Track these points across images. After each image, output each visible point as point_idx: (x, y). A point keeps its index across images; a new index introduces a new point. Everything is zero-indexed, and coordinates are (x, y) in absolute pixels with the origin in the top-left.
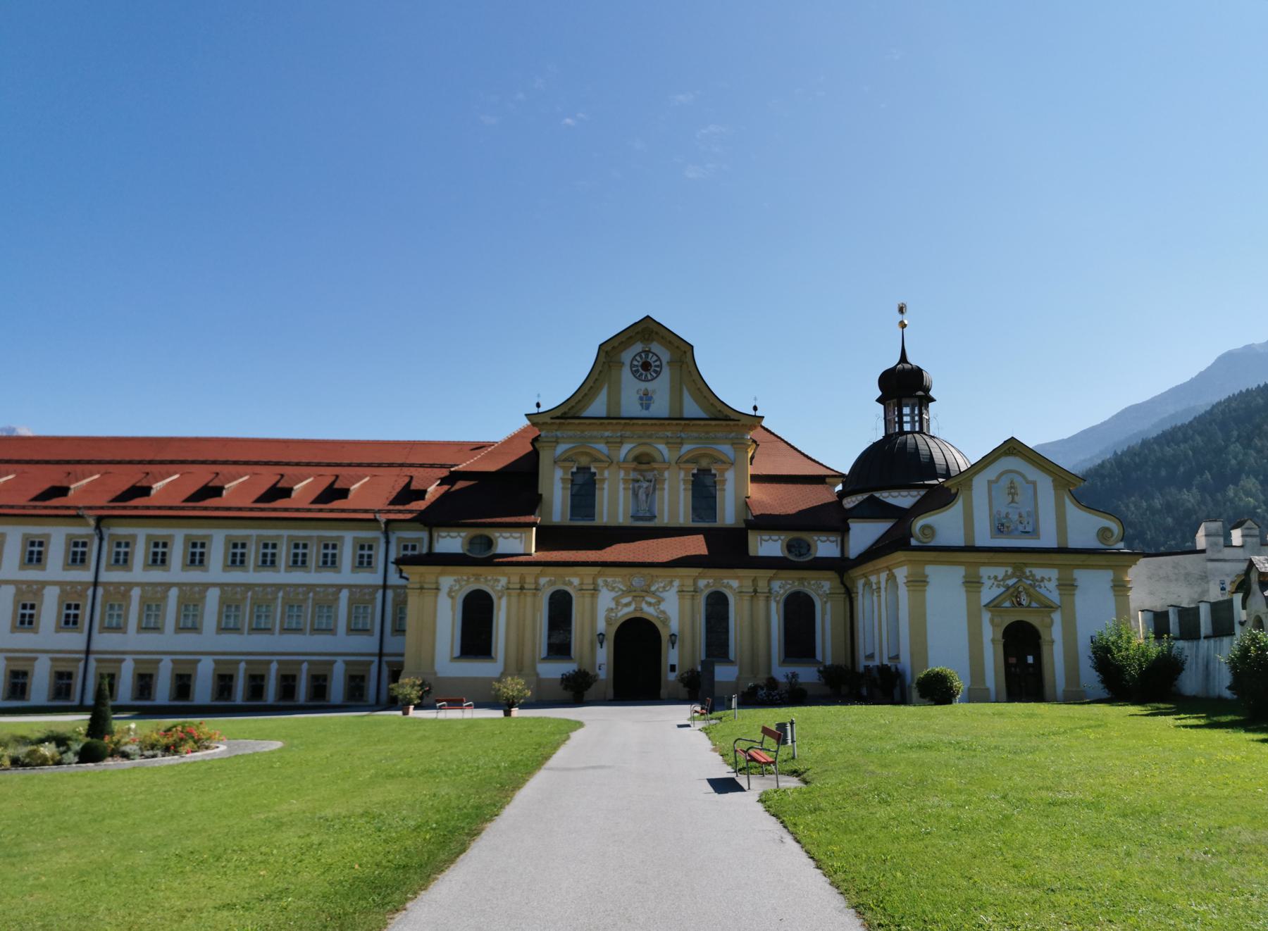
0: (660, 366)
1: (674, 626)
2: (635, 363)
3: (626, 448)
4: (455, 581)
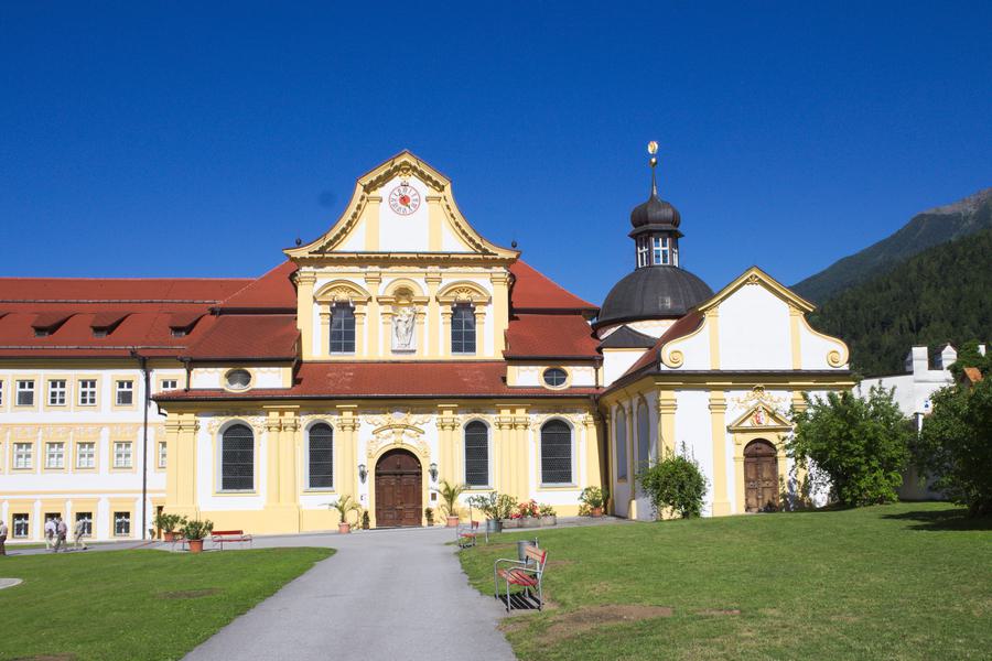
2: (393, 196)
3: (386, 280)
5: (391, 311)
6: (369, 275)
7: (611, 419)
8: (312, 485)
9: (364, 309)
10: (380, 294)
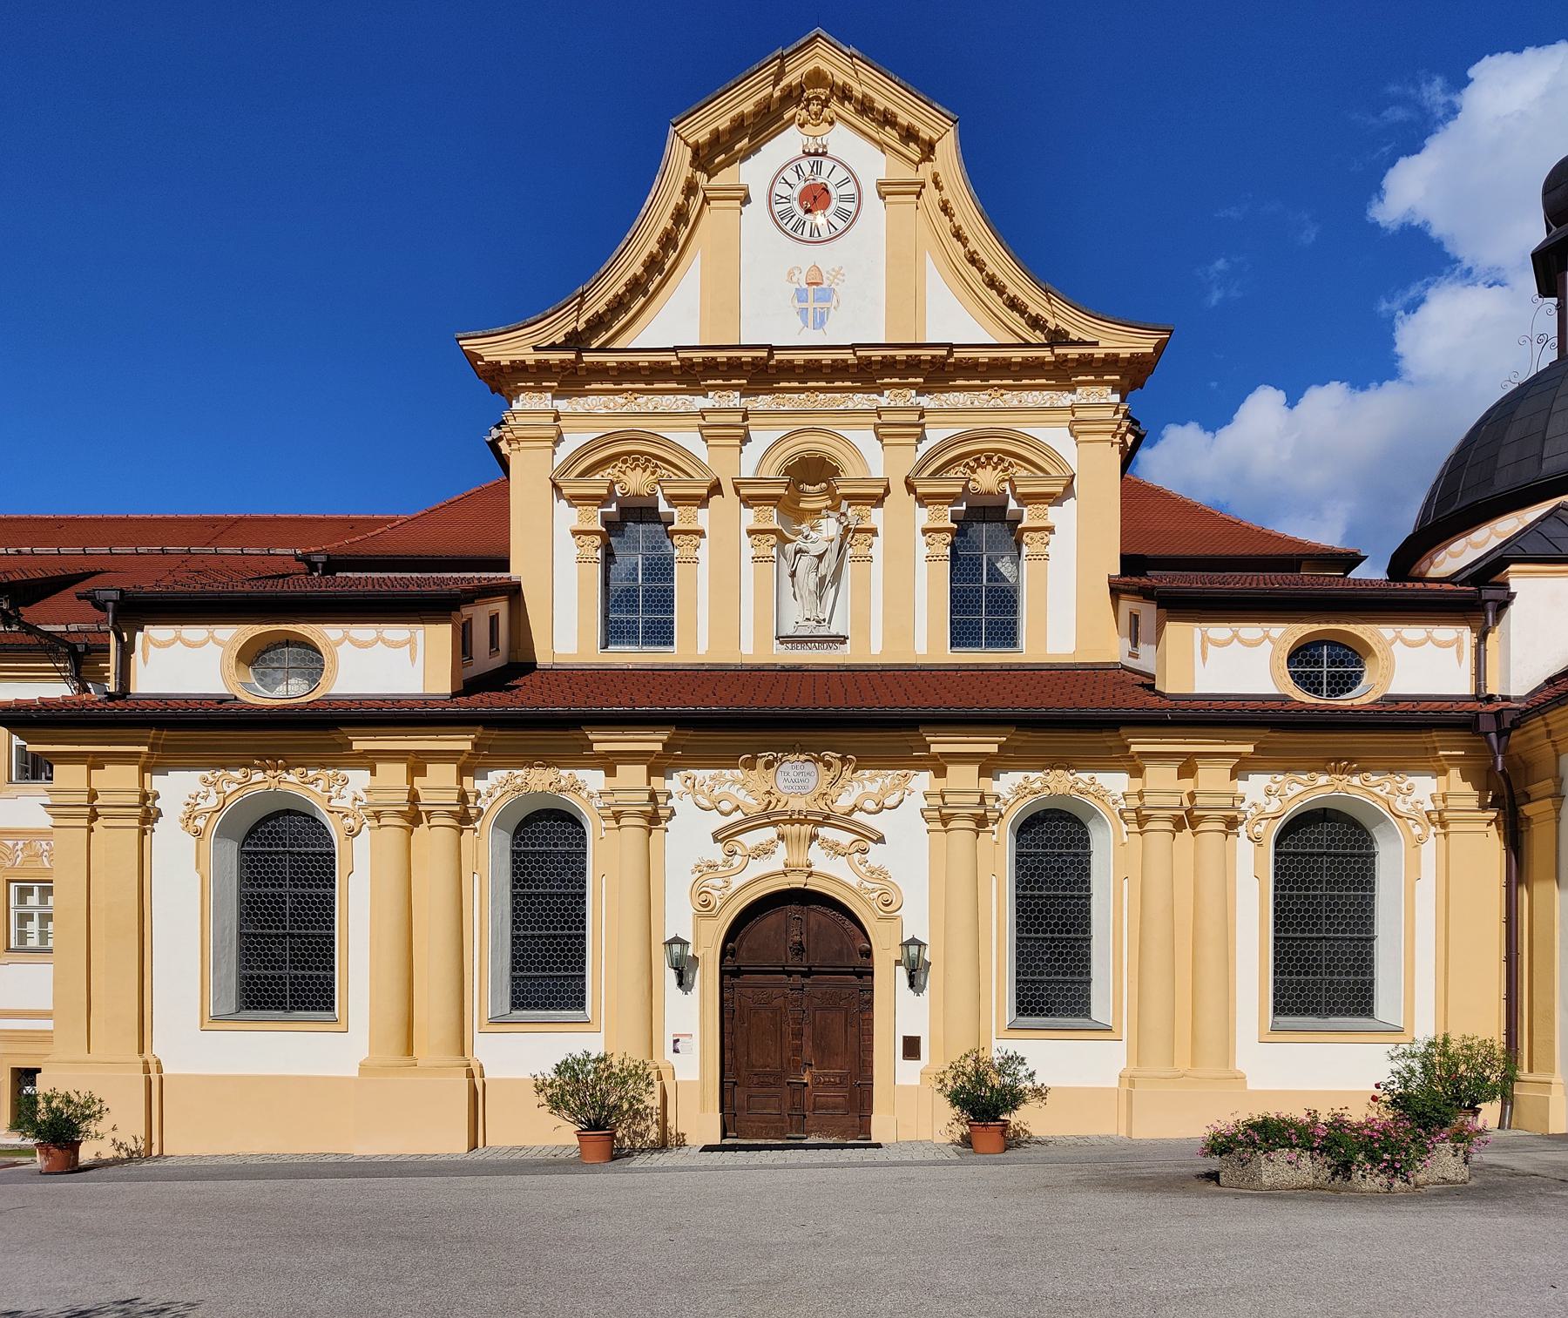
0: (857, 198)
1: (916, 921)
2: (782, 189)
3: (762, 438)
5: (774, 525)
6: (711, 419)
8: (521, 1000)
9: (702, 518)
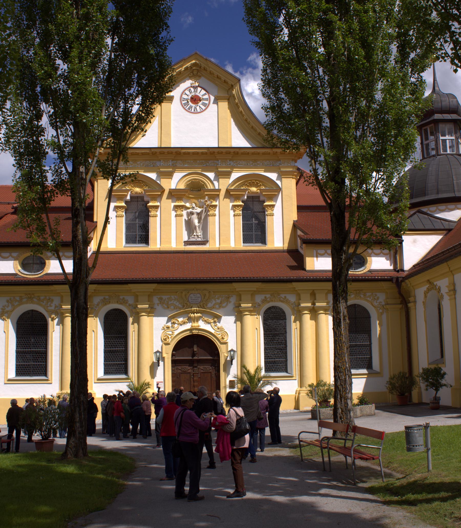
2: (185, 96)
4: (8, 301)
7: (415, 302)
10: (173, 187)
